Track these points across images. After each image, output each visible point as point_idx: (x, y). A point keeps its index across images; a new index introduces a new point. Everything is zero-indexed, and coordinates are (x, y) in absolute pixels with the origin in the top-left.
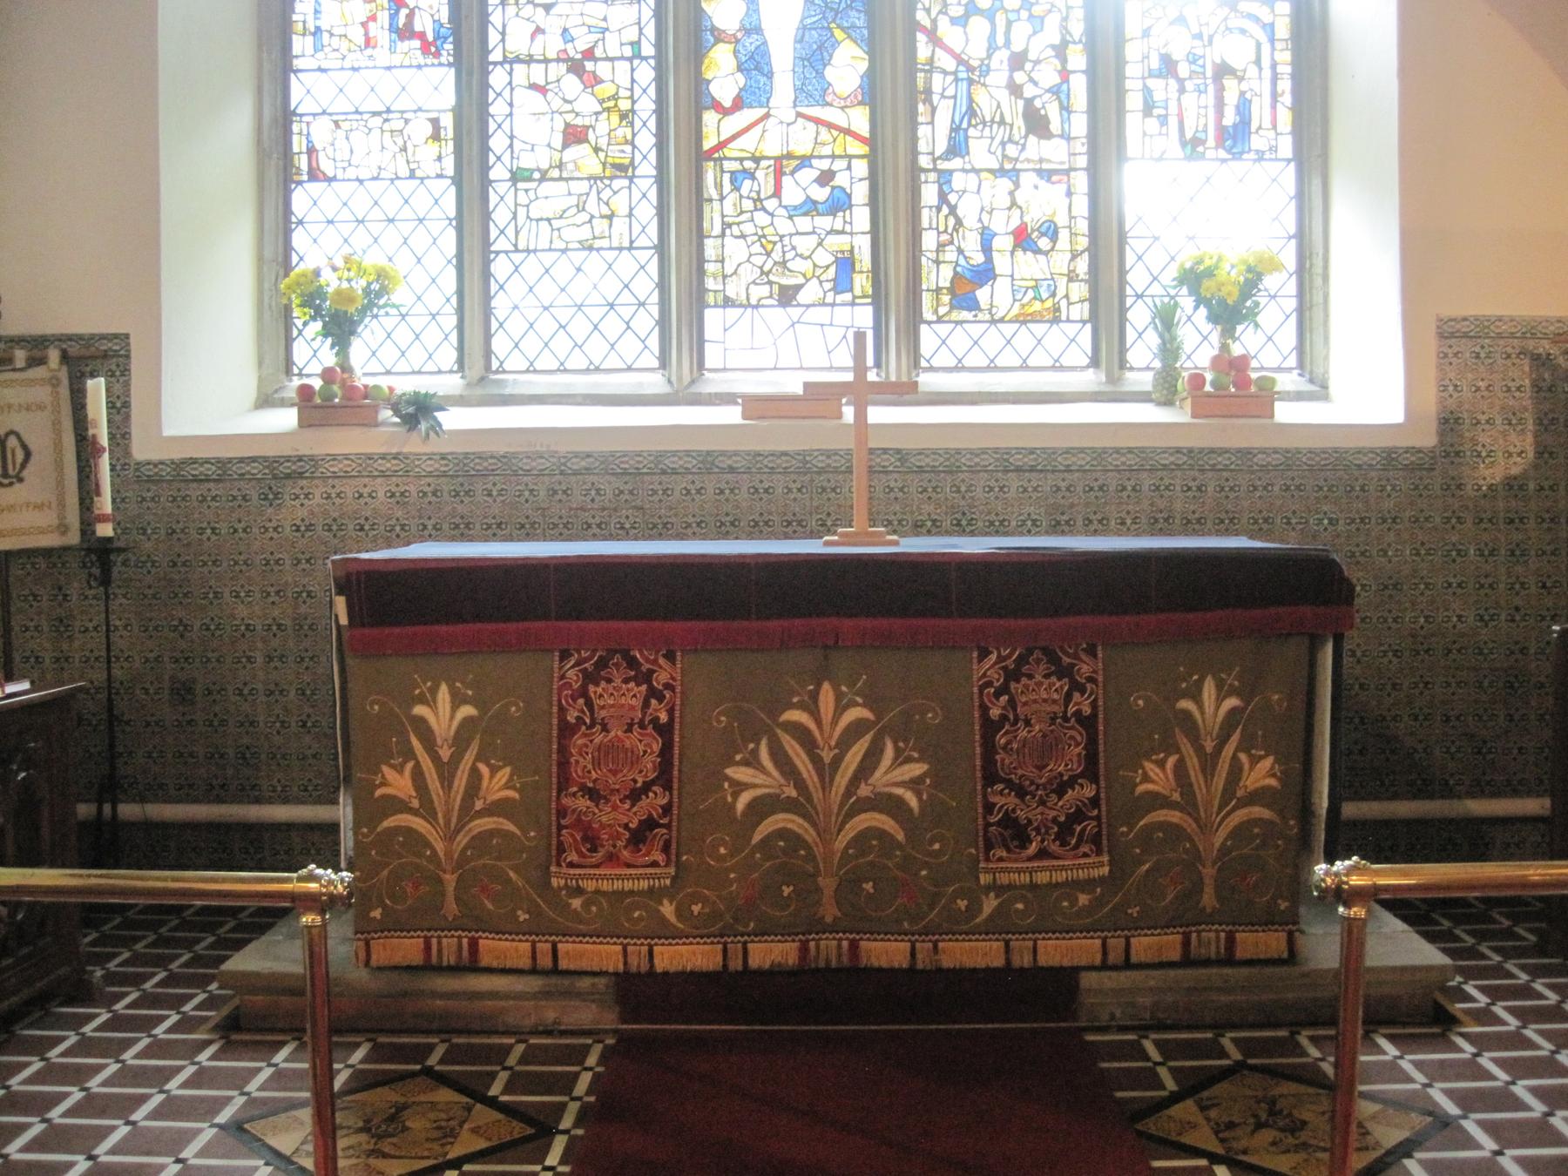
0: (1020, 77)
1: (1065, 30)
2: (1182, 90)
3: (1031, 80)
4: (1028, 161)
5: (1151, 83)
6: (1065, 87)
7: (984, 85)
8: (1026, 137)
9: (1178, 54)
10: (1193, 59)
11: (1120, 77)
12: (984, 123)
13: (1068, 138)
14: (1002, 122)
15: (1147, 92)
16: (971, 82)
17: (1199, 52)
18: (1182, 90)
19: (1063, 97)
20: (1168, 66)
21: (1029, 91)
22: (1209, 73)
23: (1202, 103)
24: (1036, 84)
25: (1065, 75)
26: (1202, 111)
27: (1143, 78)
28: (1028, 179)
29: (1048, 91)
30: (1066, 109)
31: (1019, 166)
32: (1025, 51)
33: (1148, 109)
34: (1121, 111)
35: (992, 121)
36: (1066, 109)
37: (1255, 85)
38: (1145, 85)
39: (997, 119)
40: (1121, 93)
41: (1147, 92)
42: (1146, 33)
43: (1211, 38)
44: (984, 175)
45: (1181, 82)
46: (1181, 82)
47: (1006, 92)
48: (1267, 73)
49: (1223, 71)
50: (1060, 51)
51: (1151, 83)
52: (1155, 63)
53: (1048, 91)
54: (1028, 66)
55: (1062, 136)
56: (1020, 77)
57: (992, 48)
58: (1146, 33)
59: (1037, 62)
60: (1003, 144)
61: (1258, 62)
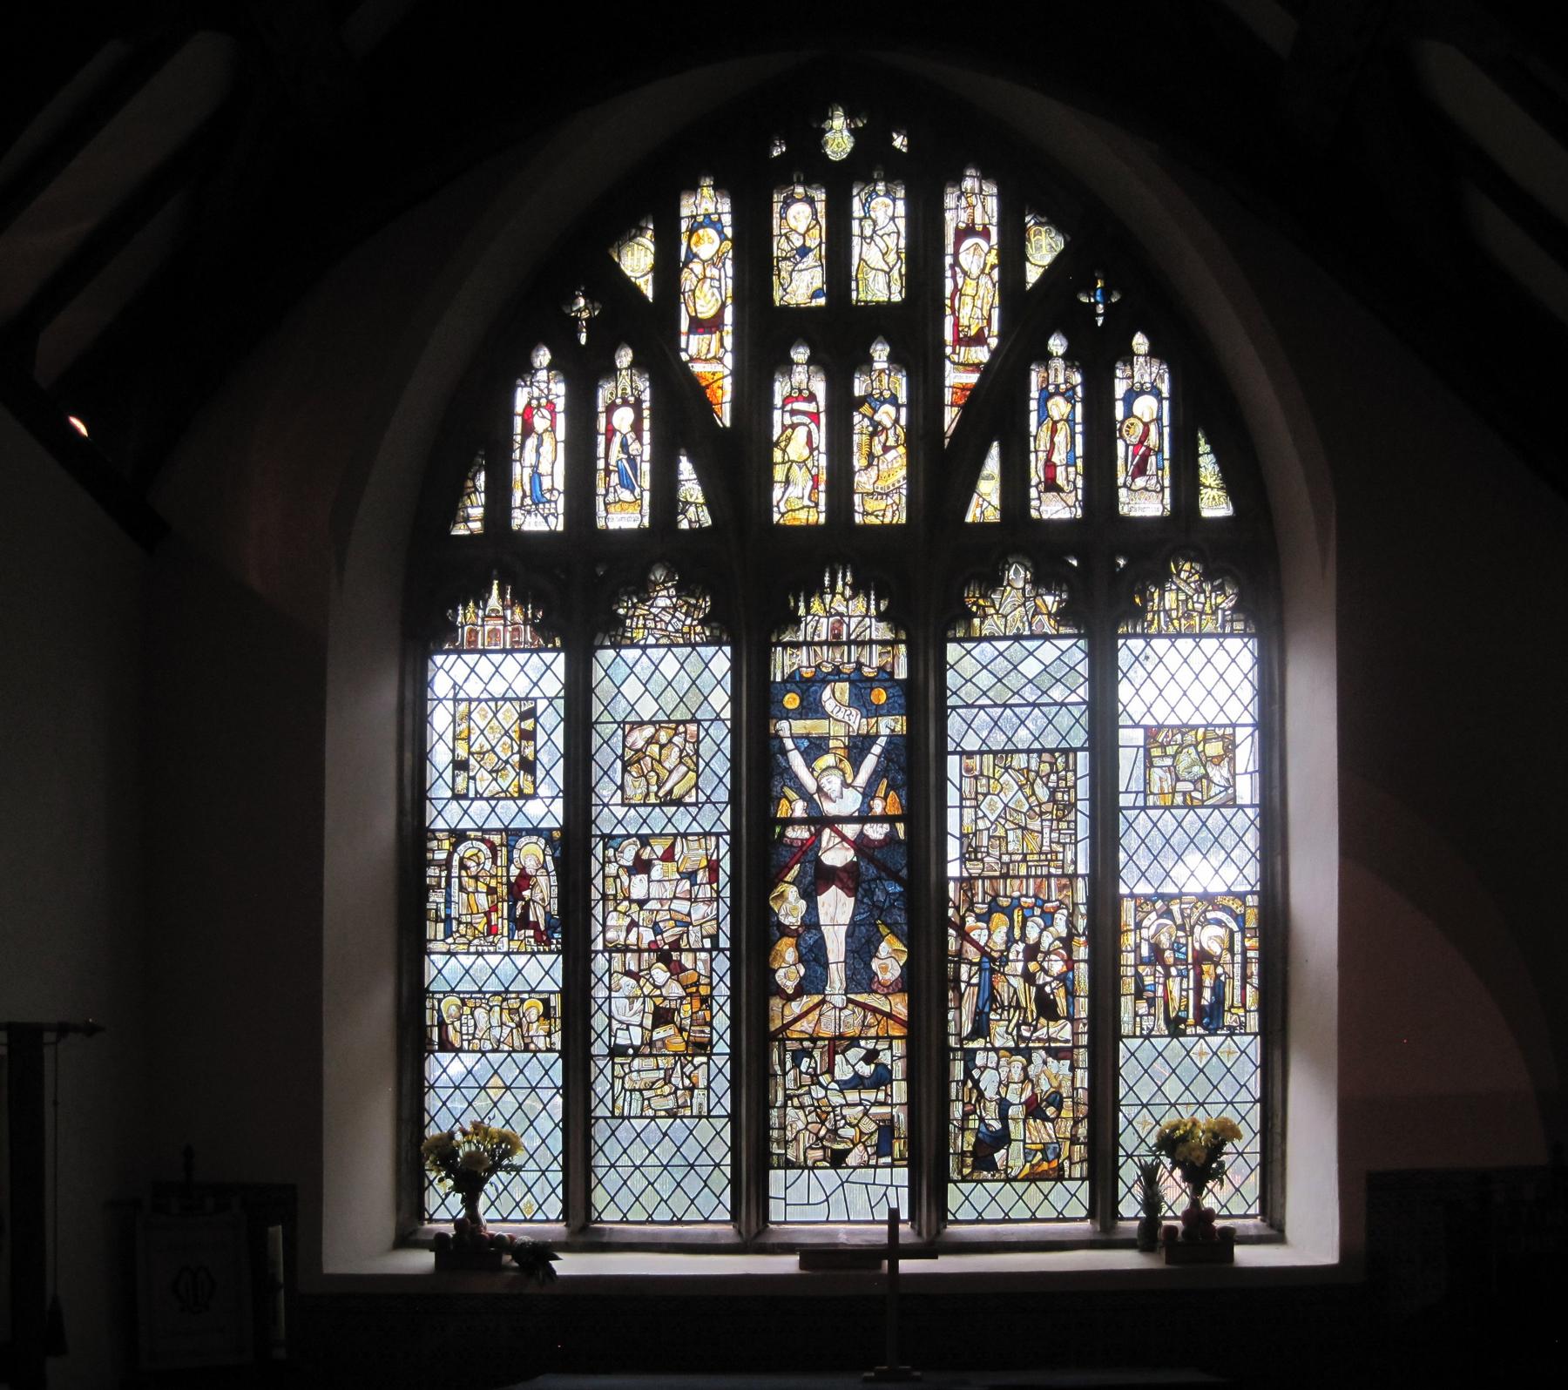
0: (1033, 966)
1: (1071, 924)
2: (1167, 976)
3: (1042, 969)
4: (1039, 1040)
5: (1141, 969)
7: (1004, 974)
8: (1037, 1019)
11: (1117, 965)
13: (1071, 1018)
14: (1018, 1007)
15: (1138, 978)
16: (992, 971)
18: (1167, 976)
20: (1157, 950)
21: (1041, 979)
24: (1046, 972)
25: (1070, 963)
27: (1136, 966)
29: (1055, 978)
30: (1071, 994)
32: (1038, 943)
33: (1139, 994)
34: (1117, 996)
35: (1010, 1006)
36: (1071, 994)
37: (1228, 968)
40: (1117, 978)
41: (1138, 978)
42: (1138, 926)
43: (1192, 928)
45: (1167, 968)
46: (1167, 968)
48: (1238, 958)
49: (1202, 957)
50: (1067, 942)
51: (1144, 970)
52: (1145, 951)
53: (1055, 978)
54: (1040, 957)
55: (1066, 1018)
56: (1033, 966)
57: (1010, 941)
58: (1138, 926)
59: (1048, 953)
60: (1018, 1026)
61: (1231, 949)
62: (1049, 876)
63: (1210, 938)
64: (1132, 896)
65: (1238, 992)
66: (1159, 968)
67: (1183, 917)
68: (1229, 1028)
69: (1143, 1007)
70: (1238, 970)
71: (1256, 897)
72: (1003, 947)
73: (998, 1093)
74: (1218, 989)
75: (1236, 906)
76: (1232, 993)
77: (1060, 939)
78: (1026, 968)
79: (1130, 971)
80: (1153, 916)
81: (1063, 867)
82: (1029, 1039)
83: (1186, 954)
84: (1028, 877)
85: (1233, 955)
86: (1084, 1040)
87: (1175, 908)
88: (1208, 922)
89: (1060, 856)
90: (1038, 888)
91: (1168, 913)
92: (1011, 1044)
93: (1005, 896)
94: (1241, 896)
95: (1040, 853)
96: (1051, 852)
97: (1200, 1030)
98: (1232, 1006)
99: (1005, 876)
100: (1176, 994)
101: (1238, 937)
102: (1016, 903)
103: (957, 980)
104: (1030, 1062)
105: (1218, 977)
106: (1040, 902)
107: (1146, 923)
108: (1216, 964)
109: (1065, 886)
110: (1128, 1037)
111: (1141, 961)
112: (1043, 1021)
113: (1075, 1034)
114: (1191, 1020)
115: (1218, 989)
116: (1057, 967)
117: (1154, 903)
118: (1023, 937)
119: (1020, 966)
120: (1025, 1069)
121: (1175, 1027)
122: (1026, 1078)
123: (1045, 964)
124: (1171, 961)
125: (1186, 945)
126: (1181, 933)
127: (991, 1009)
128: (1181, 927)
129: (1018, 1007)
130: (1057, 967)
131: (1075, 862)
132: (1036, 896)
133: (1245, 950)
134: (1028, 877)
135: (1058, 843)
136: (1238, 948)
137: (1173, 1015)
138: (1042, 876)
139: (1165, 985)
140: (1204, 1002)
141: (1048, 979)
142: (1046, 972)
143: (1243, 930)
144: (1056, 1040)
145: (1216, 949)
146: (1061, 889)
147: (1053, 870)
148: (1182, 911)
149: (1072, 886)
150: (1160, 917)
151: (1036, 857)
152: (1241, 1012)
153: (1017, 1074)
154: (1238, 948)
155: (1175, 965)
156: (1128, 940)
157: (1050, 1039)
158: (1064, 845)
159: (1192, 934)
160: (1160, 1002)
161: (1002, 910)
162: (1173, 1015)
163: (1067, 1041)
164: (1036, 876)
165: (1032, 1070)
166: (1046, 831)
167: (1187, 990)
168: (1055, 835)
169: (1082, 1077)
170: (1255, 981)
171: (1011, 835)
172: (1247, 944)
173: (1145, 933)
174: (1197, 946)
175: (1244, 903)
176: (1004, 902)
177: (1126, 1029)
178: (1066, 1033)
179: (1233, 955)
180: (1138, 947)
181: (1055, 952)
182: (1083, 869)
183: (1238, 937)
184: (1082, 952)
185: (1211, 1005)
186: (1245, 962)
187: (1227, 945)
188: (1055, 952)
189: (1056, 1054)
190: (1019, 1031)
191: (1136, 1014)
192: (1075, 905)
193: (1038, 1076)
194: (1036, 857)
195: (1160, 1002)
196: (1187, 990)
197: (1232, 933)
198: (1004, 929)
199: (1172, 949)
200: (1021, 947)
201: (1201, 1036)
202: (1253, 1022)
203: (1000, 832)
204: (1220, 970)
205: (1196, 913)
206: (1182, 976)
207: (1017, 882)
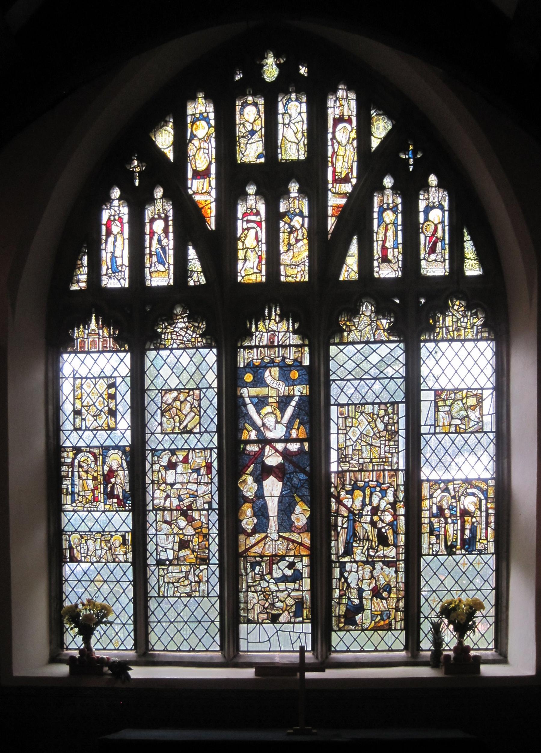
0: (375, 518)
1: (395, 496)
2: (446, 523)
3: (381, 520)
4: (379, 557)
6: (395, 522)
7: (360, 522)
8: (378, 546)
10: (451, 507)
11: (420, 517)
12: (360, 540)
13: (396, 546)
14: (368, 539)
15: (431, 524)
17: (454, 504)
18: (446, 523)
19: (394, 527)
22: (458, 515)
23: (455, 528)
24: (383, 521)
25: (395, 516)
26: (455, 532)
27: (430, 518)
28: (378, 566)
29: (388, 525)
30: (396, 533)
31: (375, 559)
32: (378, 506)
33: (431, 533)
34: (420, 533)
35: (364, 539)
36: (396, 533)
37: (478, 519)
38: (430, 520)
39: (366, 538)
40: (420, 525)
41: (431, 524)
42: (431, 496)
43: (460, 497)
44: (360, 564)
45: (446, 519)
47: (370, 526)
48: (484, 514)
49: (465, 513)
50: (393, 505)
52: (435, 510)
53: (388, 525)
56: (375, 518)
57: (364, 505)
58: (431, 496)
59: (383, 511)
60: (368, 549)
61: (480, 509)
62: (384, 470)
64: (428, 480)
66: (442, 519)
67: (455, 492)
69: (433, 539)
70: (484, 520)
71: (493, 481)
72: (360, 508)
73: (358, 585)
74: (473, 530)
77: (390, 504)
78: (372, 519)
79: (427, 521)
80: (439, 491)
81: (391, 466)
82: (374, 556)
83: (456, 511)
84: (373, 471)
85: (481, 512)
86: (402, 557)
87: (451, 487)
88: (468, 494)
89: (390, 460)
90: (378, 477)
91: (447, 490)
92: (365, 559)
93: (361, 481)
95: (379, 458)
96: (385, 457)
99: (361, 470)
100: (451, 532)
101: (484, 502)
102: (367, 485)
103: (336, 525)
104: (374, 568)
105: (473, 523)
106: (380, 485)
107: (435, 495)
108: (472, 517)
109: (392, 476)
111: (432, 515)
112: (381, 547)
113: (398, 553)
114: (459, 546)
116: (388, 518)
117: (439, 484)
118: (371, 503)
119: (369, 518)
120: (371, 572)
121: (450, 550)
122: (372, 577)
123: (382, 517)
124: (448, 515)
125: (456, 507)
126: (453, 500)
127: (354, 541)
128: (454, 497)
129: (368, 539)
130: (388, 518)
131: (397, 463)
132: (377, 481)
133: (487, 509)
134: (373, 471)
135: (389, 452)
136: (484, 508)
137: (449, 544)
138: (380, 470)
139: (445, 528)
140: (465, 537)
141: (384, 525)
142: (383, 521)
144: (388, 557)
145: (472, 508)
146: (390, 477)
147: (386, 467)
148: (454, 488)
149: (396, 475)
150: (442, 492)
151: (377, 460)
153: (367, 575)
154: (484, 508)
155: (450, 517)
156: (426, 504)
157: (385, 557)
158: (392, 453)
159: (459, 500)
160: (442, 537)
161: (360, 488)
162: (449, 544)
163: (394, 557)
164: (377, 470)
165: (375, 573)
166: (383, 446)
167: (457, 530)
168: (387, 448)
169: (402, 577)
171: (364, 448)
172: (489, 506)
173: (435, 500)
174: (462, 507)
175: (487, 484)
176: (361, 484)
177: (425, 551)
178: (393, 553)
179: (481, 512)
180: (431, 507)
181: (387, 510)
182: (402, 466)
183: (484, 502)
184: (402, 511)
185: (469, 538)
186: (487, 516)
187: (478, 507)
188: (387, 510)
189: (388, 564)
190: (368, 552)
191: (430, 543)
192: (398, 485)
193: (378, 576)
194: (377, 460)
195: (442, 537)
196: (457, 530)
197: (480, 500)
198: (361, 498)
199: (449, 509)
200: (369, 508)
203: (359, 447)
204: (474, 520)
205: (462, 489)
207: (367, 473)
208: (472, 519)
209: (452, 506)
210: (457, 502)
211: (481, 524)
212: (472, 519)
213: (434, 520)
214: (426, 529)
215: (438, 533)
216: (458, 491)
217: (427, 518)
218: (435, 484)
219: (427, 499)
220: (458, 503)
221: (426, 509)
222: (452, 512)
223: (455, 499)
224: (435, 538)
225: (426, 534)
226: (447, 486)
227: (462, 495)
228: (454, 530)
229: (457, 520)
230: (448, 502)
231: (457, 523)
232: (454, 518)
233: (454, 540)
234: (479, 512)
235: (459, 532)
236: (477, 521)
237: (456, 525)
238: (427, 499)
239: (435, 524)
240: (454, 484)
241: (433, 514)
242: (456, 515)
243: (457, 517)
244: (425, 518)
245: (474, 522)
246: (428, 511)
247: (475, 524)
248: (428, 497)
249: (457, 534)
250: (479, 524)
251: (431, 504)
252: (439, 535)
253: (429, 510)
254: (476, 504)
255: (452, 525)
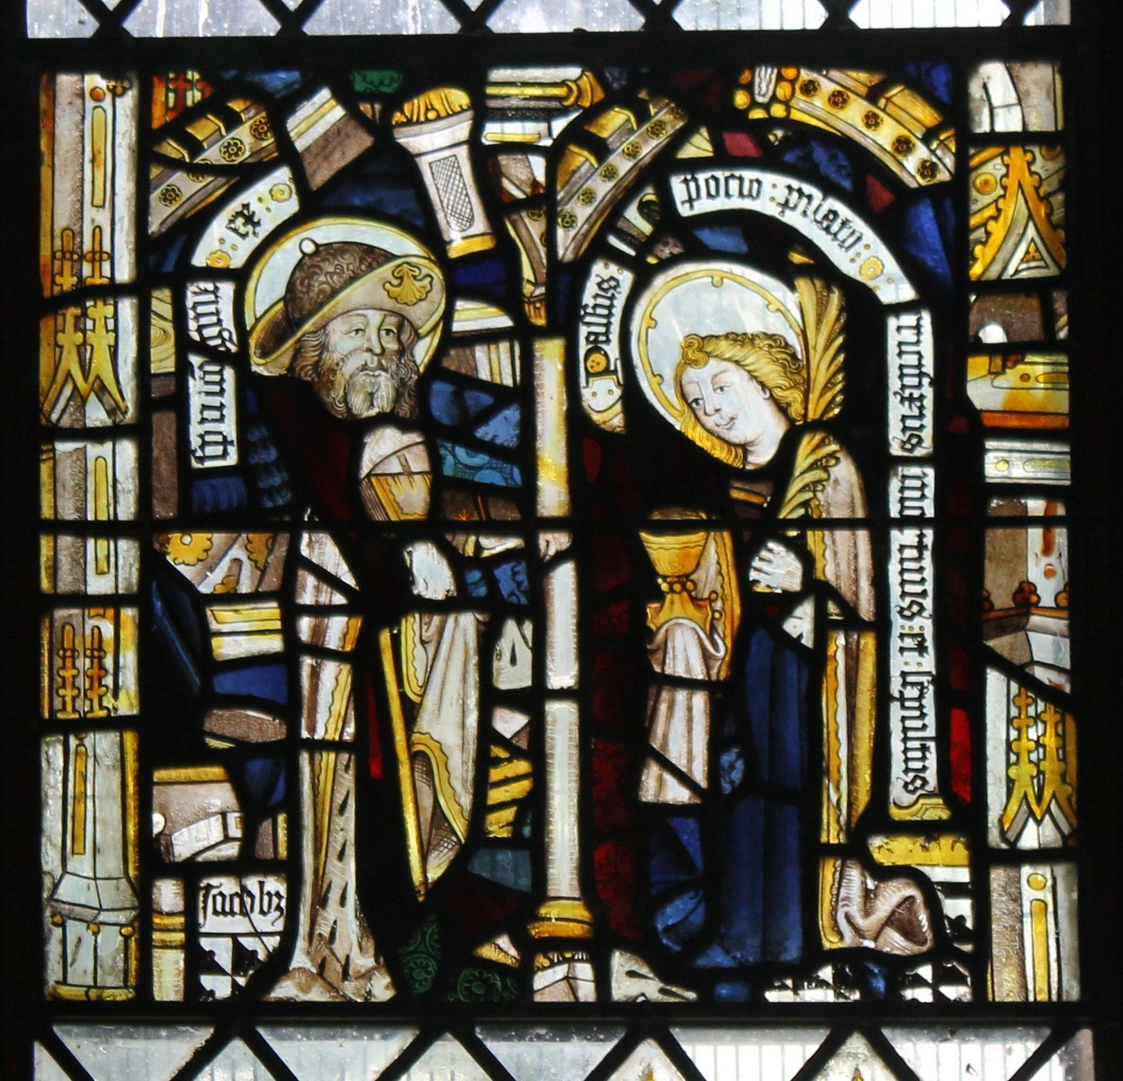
5: (184, 551)
9: (356, 351)
10: (444, 404)
17: (496, 364)
18: (383, 597)
20: (302, 443)
22: (552, 494)
26: (509, 723)
27: (146, 530)
33: (168, 731)
37: (842, 557)
38: (154, 566)
42: (166, 260)
43: (566, 280)
48: (913, 491)
49: (647, 471)
52: (214, 421)
58: (166, 260)
61: (857, 423)
63: (716, 349)
65: (915, 726)
66: (324, 551)
68: (855, 964)
69: (201, 815)
70: (913, 564)
71: (1040, 76)
74: (767, 689)
75: (893, 127)
76: (878, 721)
79: (112, 568)
80: (272, 198)
83: (524, 454)
85: (876, 467)
87: (436, 137)
88: (691, 239)
91: (383, 182)
94: (932, 62)
97: (632, 981)
98: (876, 818)
101: (911, 342)
105: (763, 611)
107: (219, 243)
110: (95, 1013)
111: (182, 497)
114: (564, 908)
115: (767, 689)
117: (278, 110)
121: (448, 947)
124: (411, 498)
125: (523, 394)
126: (474, 316)
136: (908, 419)
137: (428, 867)
140: (659, 787)
143: (948, 294)
145: (742, 417)
148: (485, 162)
150: (313, 205)
152: (947, 863)
154: (908, 419)
155: (433, 528)
156: (105, 349)
159: (565, 318)
160: (330, 783)
162: (428, 867)
167: (532, 700)
170: (1047, 644)
172: (985, 391)
173: (212, 309)
174: (603, 399)
175: (955, 113)
177: (83, 957)
179: (876, 467)
180: (162, 400)
183: (911, 342)
185: (710, 800)
186: (968, 517)
187: (825, 395)
191: (151, 858)
195: (330, 783)
196: (532, 700)
197: (863, 317)
199: (415, 414)
201: (637, 1024)
202: (1037, 938)
204: (777, 569)
206: (501, 599)
208: (743, 558)
209: (467, 382)
210: (523, 335)
211: (881, 626)
212: (743, 558)
213: (208, 562)
214: (106, 663)
215: (260, 726)
216: (544, 201)
217: (111, 529)
218: (215, 105)
219: (112, 291)
220: (550, 354)
221: (97, 416)
222: (458, 458)
223: (504, 292)
224: (221, 796)
225: (104, 743)
226: (382, 131)
227: (597, 249)
228: (491, 698)
229: (540, 569)
230: (404, 329)
231: (535, 610)
232: (494, 545)
233: (498, 825)
234: (845, 471)
235: (563, 719)
236: (816, 588)
237: (514, 636)
238: (112, 291)
239: (223, 618)
240: (482, 112)
241: (188, 477)
242: (527, 493)
243: (531, 525)
244: (84, 529)
245: (786, 602)
246: (127, 450)
247: (800, 624)
248: (124, 272)
249: (534, 748)
250: (852, 622)
251: (163, 359)
252: (289, 749)
253: (140, 432)
254: (796, 366)
255: (466, 624)
